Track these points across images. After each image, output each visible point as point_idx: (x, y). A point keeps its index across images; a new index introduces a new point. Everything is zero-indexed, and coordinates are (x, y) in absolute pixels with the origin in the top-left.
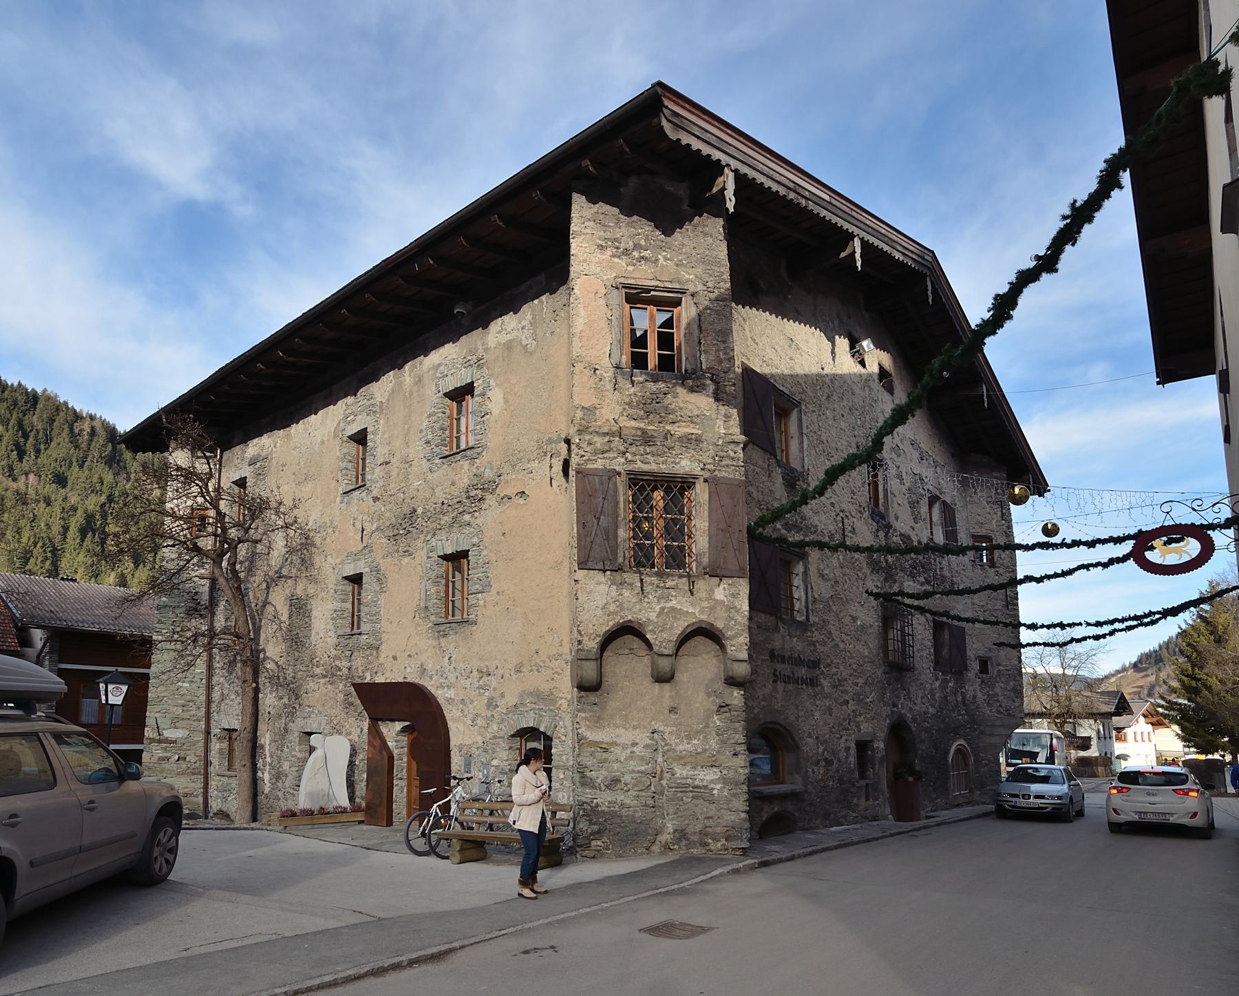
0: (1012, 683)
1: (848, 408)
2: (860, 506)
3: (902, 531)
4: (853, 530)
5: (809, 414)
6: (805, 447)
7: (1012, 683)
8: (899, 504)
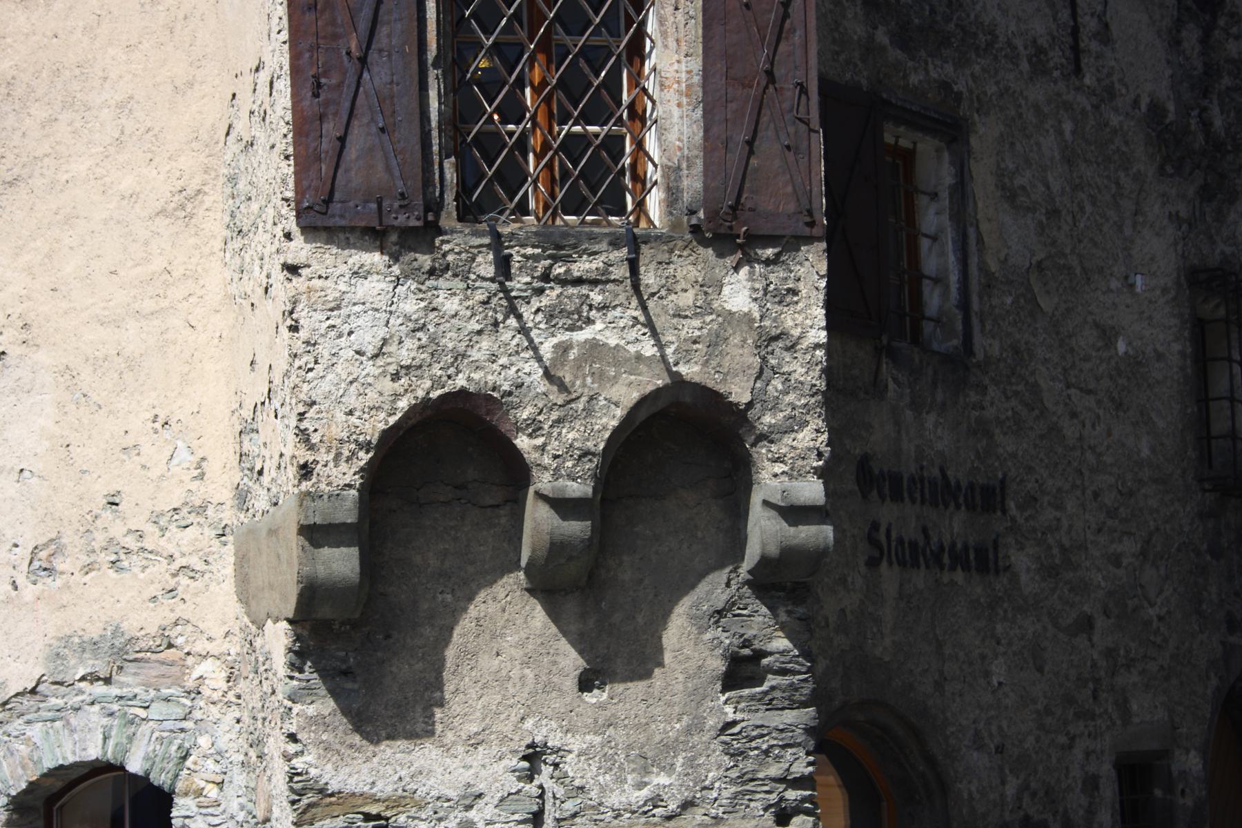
4: (1104, 34)
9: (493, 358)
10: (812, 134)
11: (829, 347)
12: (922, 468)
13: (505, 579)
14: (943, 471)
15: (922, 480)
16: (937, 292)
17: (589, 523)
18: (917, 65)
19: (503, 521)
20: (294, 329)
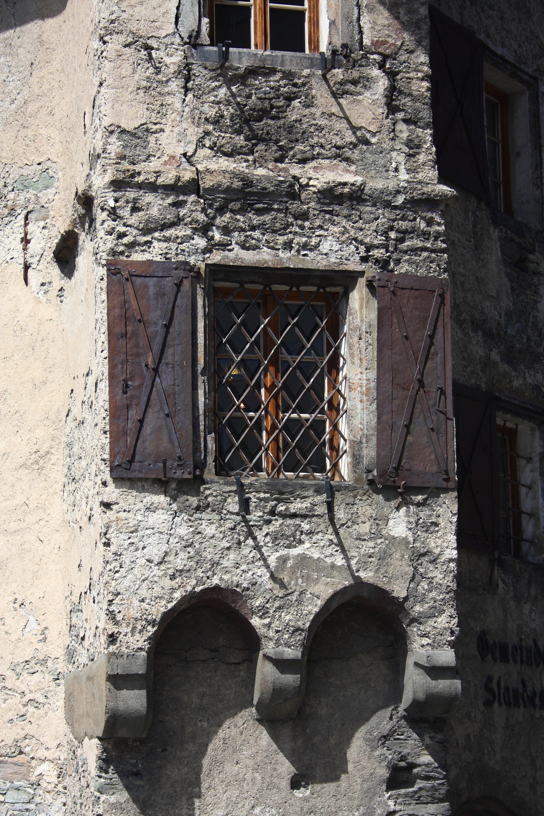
9: (237, 565)
10: (448, 421)
11: (459, 561)
12: (521, 640)
13: (243, 713)
14: (535, 642)
15: (521, 648)
16: (531, 523)
17: (299, 676)
18: (518, 374)
19: (242, 673)
20: (107, 544)
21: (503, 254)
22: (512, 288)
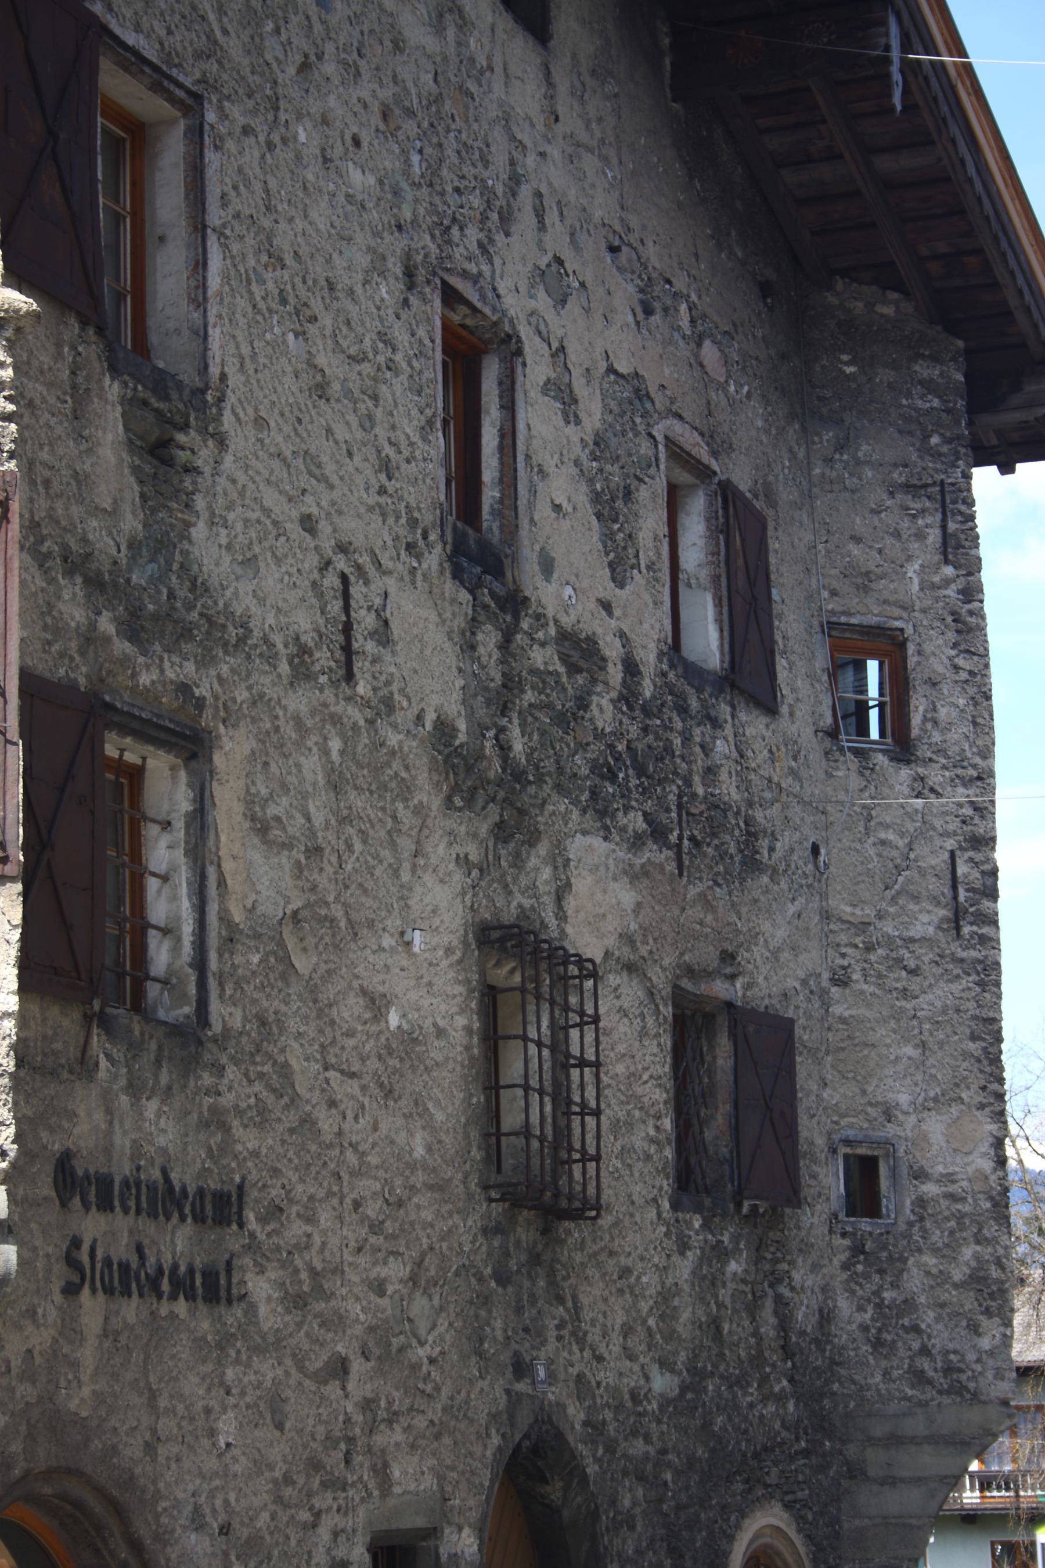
0: (967, 1253)
1: (376, 107)
2: (413, 523)
3: (567, 621)
4: (383, 633)
5: (230, 145)
6: (214, 282)
7: (967, 1253)
8: (557, 508)
10: (9, 746)
11: (22, 1018)
12: (138, 1169)
14: (164, 1172)
15: (138, 1184)
16: (166, 945)
21: (127, 429)
22: (142, 495)
